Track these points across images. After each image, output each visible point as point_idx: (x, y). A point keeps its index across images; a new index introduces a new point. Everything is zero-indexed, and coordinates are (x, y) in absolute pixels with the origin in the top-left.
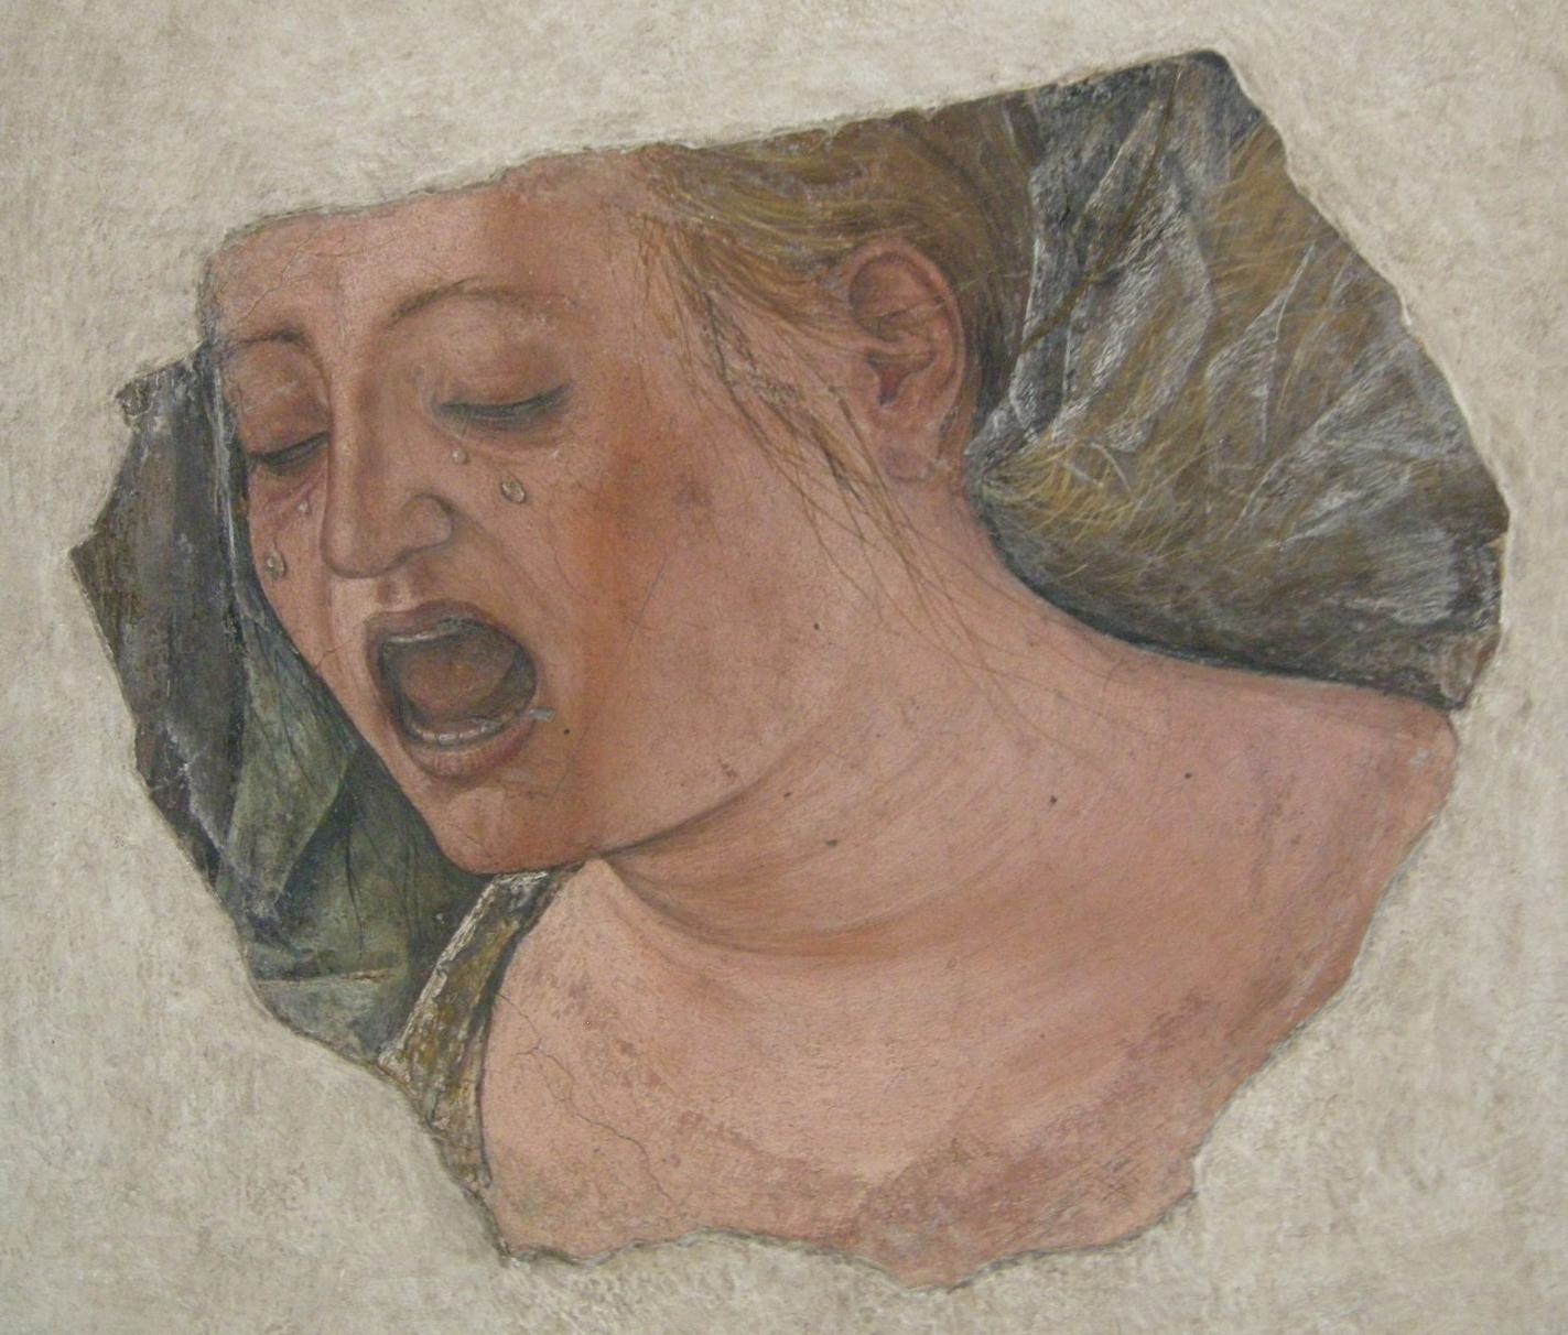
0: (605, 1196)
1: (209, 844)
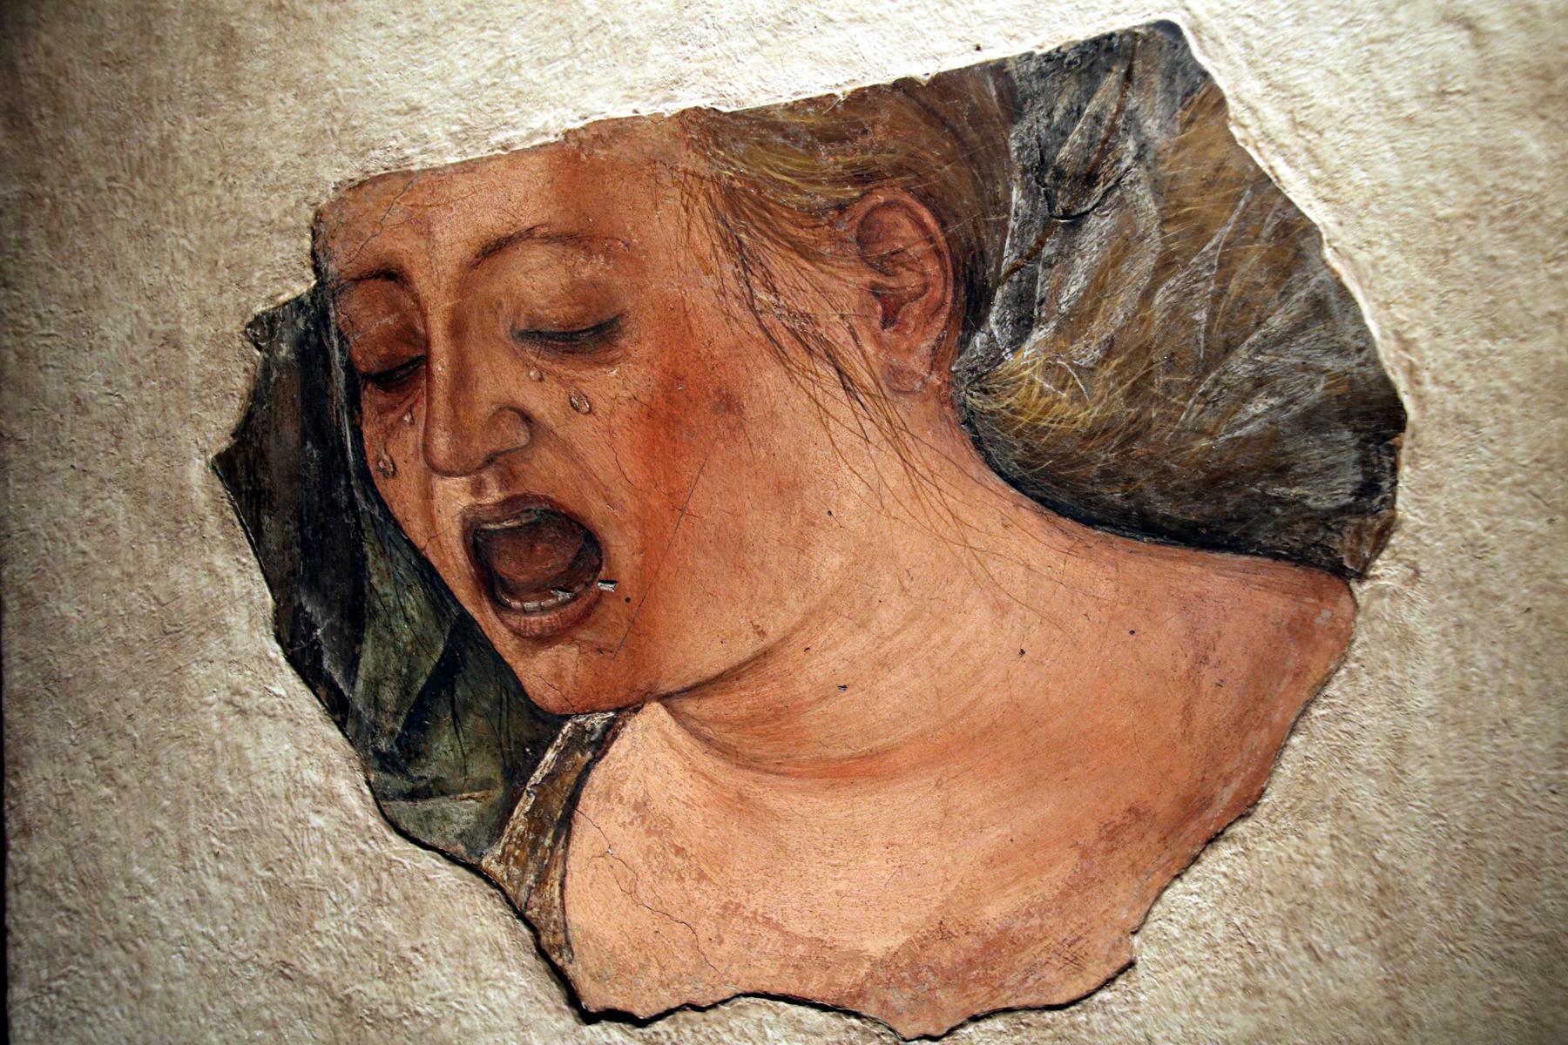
0: (663, 968)
1: (340, 692)
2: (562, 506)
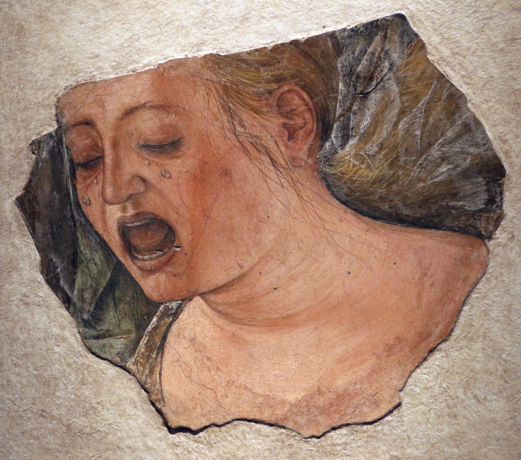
0: (203, 408)
1: (67, 295)
2: (159, 216)
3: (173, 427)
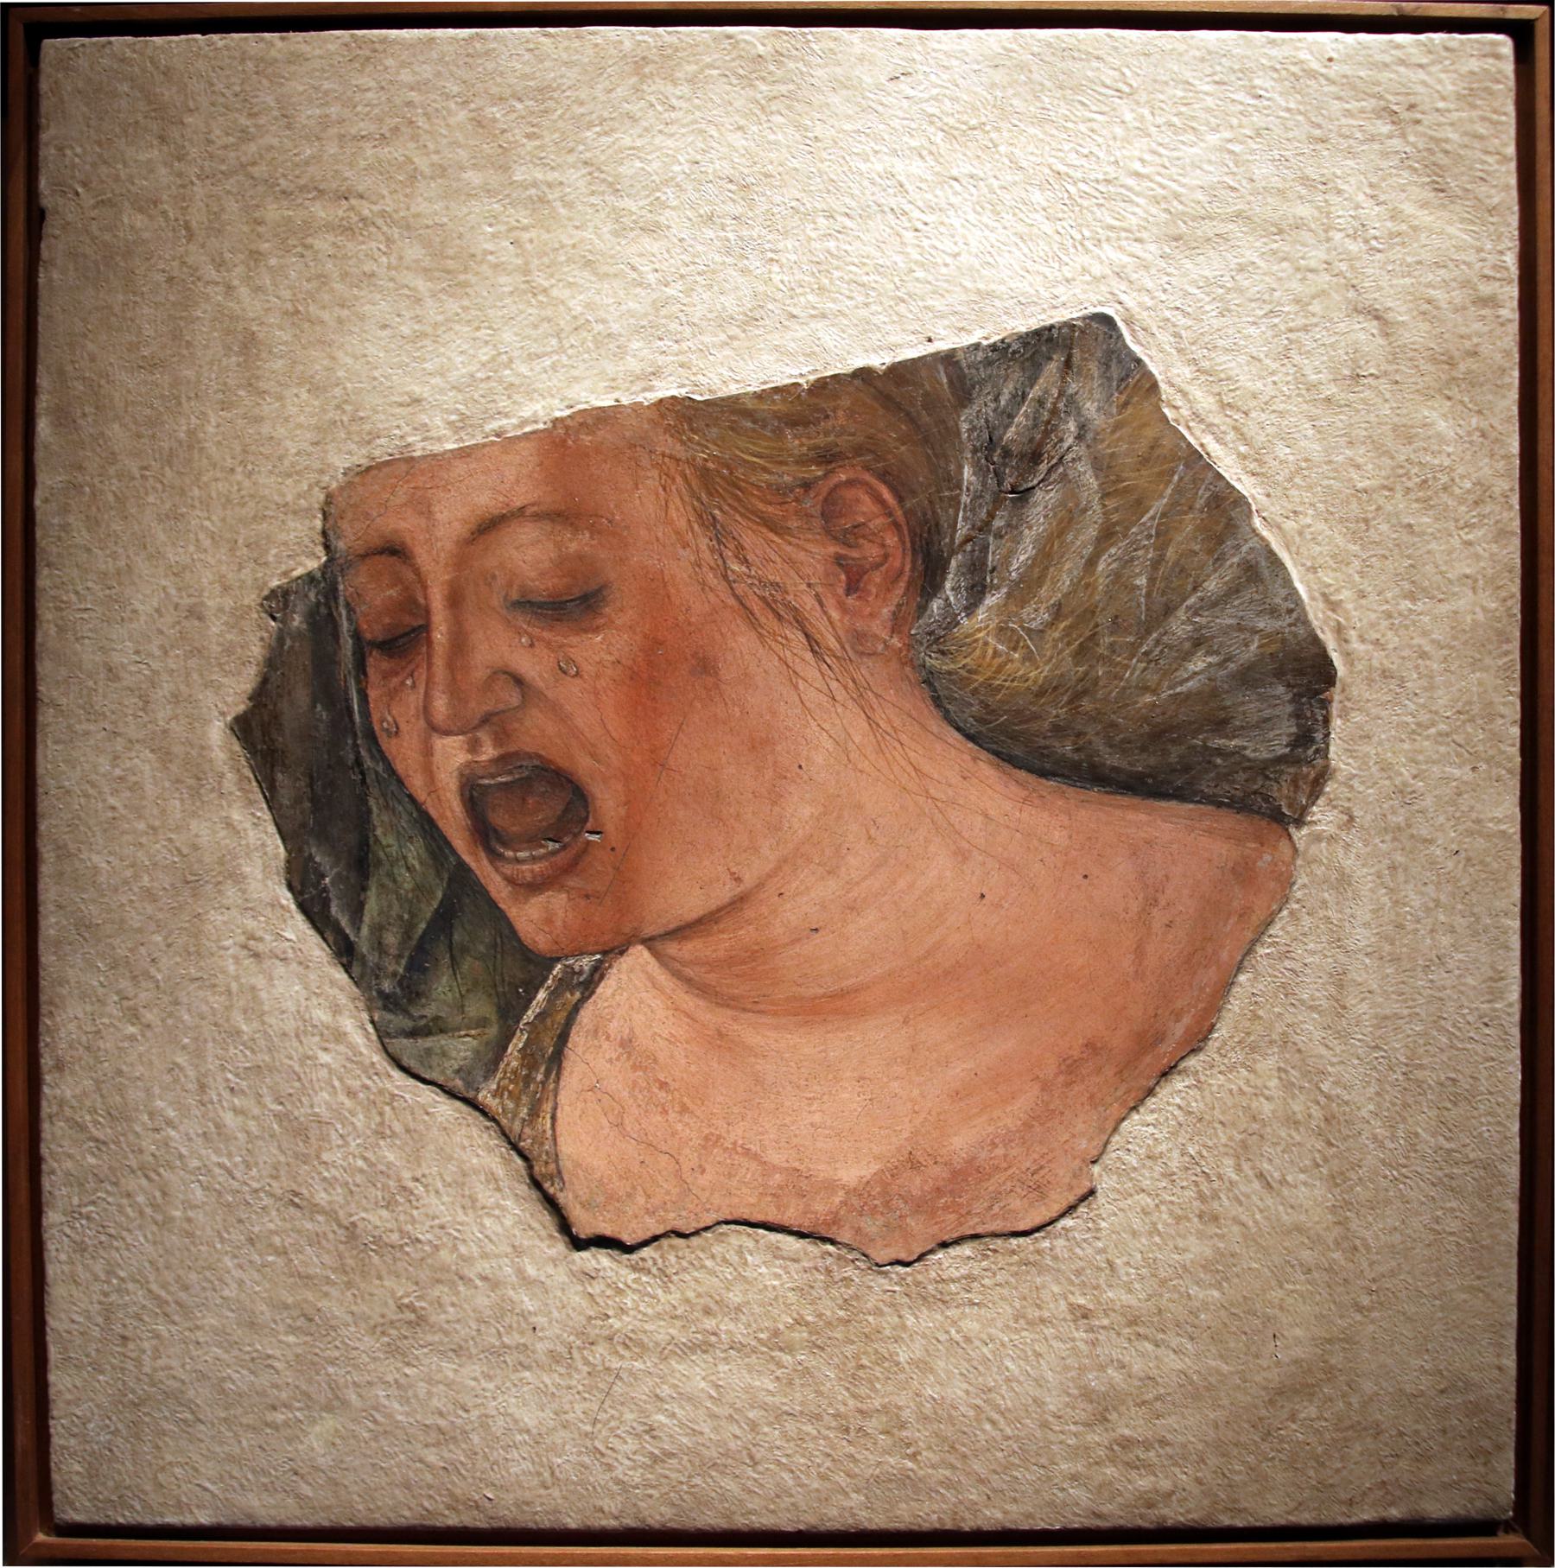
1: (346, 937)
2: (550, 761)
3: (583, 1236)
